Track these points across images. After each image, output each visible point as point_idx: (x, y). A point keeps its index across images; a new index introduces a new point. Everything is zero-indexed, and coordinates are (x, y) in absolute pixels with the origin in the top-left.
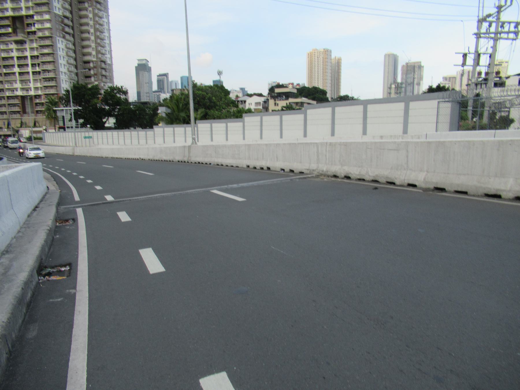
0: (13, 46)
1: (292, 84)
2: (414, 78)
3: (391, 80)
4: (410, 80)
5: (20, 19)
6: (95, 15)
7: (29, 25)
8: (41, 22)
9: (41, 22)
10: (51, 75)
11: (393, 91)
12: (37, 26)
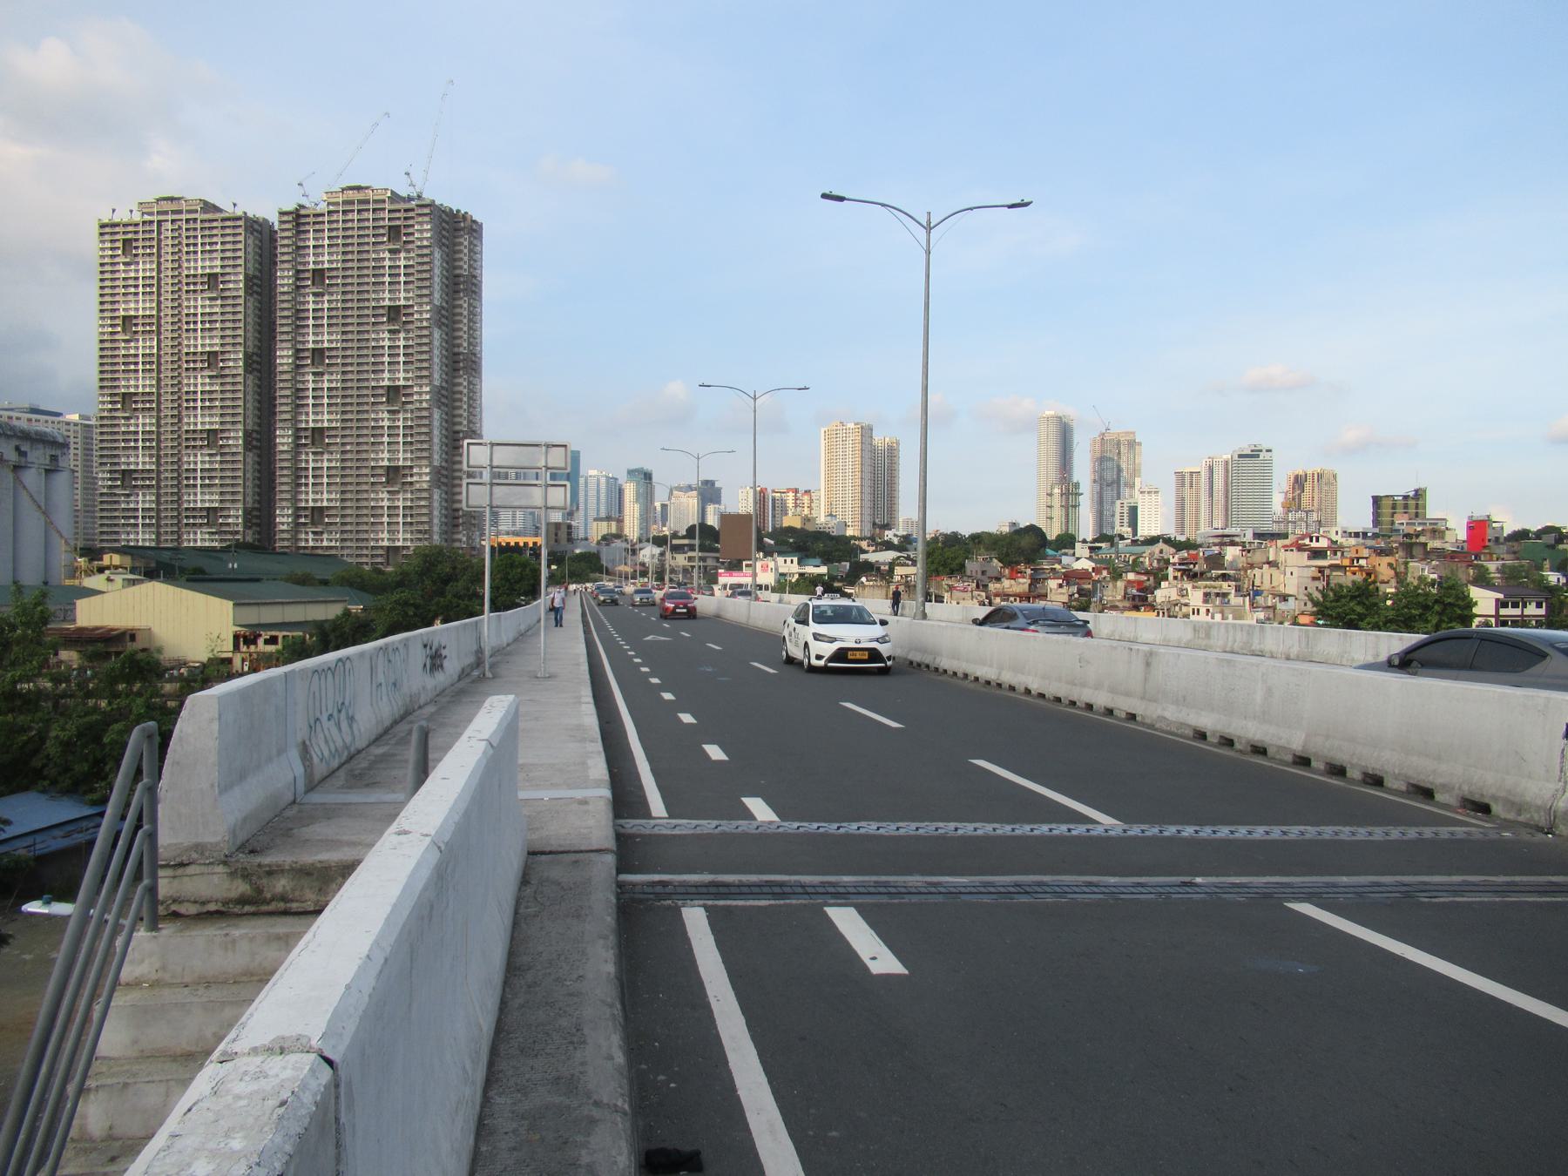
0: (385, 495)
1: (796, 491)
2: (1119, 470)
3: (1053, 474)
4: (1110, 476)
5: (397, 468)
7: (405, 476)
8: (420, 475)
9: (420, 475)
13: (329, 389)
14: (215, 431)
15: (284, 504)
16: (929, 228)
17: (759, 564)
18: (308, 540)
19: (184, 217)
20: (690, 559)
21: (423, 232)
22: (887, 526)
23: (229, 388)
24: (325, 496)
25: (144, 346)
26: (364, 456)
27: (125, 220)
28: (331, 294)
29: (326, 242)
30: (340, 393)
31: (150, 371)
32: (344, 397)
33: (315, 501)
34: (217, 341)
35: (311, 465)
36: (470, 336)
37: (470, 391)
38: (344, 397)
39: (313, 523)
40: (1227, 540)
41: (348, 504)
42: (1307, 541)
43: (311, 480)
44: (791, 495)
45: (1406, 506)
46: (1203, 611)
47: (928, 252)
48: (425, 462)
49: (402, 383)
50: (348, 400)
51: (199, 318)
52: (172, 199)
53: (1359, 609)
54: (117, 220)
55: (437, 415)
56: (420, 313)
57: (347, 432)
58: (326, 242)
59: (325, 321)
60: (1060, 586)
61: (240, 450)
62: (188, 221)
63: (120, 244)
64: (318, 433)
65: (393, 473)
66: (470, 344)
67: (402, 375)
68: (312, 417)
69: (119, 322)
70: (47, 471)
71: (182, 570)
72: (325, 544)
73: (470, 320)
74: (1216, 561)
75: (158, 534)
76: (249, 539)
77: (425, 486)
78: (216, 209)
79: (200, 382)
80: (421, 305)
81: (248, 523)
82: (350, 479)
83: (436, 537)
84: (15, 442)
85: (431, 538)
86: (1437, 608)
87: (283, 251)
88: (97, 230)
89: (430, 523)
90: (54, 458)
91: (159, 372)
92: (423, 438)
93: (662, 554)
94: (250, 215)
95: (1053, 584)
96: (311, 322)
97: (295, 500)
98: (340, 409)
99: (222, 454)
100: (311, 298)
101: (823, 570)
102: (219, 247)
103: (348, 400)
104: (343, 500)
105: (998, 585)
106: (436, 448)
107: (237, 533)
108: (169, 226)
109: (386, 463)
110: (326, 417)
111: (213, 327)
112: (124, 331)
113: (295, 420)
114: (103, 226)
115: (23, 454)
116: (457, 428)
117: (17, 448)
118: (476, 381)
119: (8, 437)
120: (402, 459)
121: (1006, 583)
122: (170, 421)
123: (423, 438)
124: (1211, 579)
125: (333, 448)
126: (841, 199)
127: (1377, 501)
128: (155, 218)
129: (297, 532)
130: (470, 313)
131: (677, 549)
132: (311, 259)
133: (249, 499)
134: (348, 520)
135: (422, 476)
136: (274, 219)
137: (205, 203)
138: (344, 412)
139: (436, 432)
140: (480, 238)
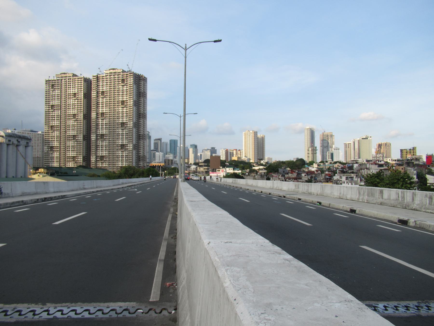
0: (120, 152)
1: (236, 150)
2: (328, 143)
3: (309, 145)
4: (325, 145)
5: (124, 145)
6: (143, 142)
9: (130, 146)
10: (131, 161)
11: (310, 152)
12: (128, 147)
13: (106, 123)
14: (75, 135)
15: (93, 155)
16: (186, 49)
17: (221, 170)
18: (100, 165)
19: (68, 78)
20: (204, 169)
21: (131, 80)
22: (262, 160)
23: (79, 124)
24: (104, 153)
25: (57, 113)
26: (115, 141)
27: (52, 79)
28: (106, 98)
29: (105, 84)
30: (108, 124)
31: (58, 119)
32: (109, 125)
33: (101, 154)
34: (76, 111)
35: (100, 144)
36: (144, 108)
37: (144, 123)
38: (109, 125)
39: (101, 160)
40: (355, 162)
41: (110, 155)
42: (378, 162)
43: (100, 148)
44: (235, 151)
45: (410, 152)
46: (346, 182)
47: (186, 57)
48: (131, 143)
49: (125, 121)
50: (110, 126)
51: (71, 105)
52: (65, 73)
53: (378, 180)
54: (50, 79)
55: (134, 130)
56: (130, 102)
57: (110, 135)
58: (105, 84)
59: (105, 105)
60: (305, 175)
61: (82, 140)
62: (69, 79)
63: (51, 86)
64: (102, 135)
65: (123, 146)
66: (144, 110)
67: (125, 119)
68: (101, 131)
69: (50, 106)
70: (26, 147)
71: (61, 173)
72: (104, 166)
73: (144, 104)
74: (351, 168)
75: (60, 164)
76: (84, 165)
77: (131, 149)
78: (76, 76)
79: (71, 122)
80: (130, 100)
81: (84, 160)
82: (111, 148)
83: (134, 164)
84: (17, 139)
85: (133, 164)
86: (401, 180)
87: (94, 86)
88: (45, 82)
89: (132, 159)
90: (27, 143)
91: (61, 120)
92: (131, 136)
93: (197, 168)
94: (85, 77)
95: (303, 175)
96: (101, 105)
97: (96, 154)
98: (108, 129)
99: (77, 142)
100: (101, 99)
101: (240, 171)
102: (77, 86)
103: (110, 126)
104: (109, 154)
105: (287, 175)
106: (134, 139)
107: (80, 163)
108: (64, 81)
109: (121, 143)
110: (105, 131)
111: (75, 107)
112: (52, 109)
113: (96, 132)
114: (46, 81)
115: (19, 142)
116: (140, 133)
117: (17, 140)
118: (145, 120)
119: (15, 137)
120: (125, 142)
121: (290, 175)
122: (63, 133)
123: (131, 136)
124: (349, 173)
125: (106, 139)
126: (155, 40)
127: (401, 151)
128: (60, 79)
129: (97, 163)
130: (144, 102)
131: (201, 166)
132: (101, 88)
133: (84, 154)
134: (110, 159)
135: (130, 147)
136: (91, 78)
137: (73, 74)
138: (109, 130)
139: (134, 135)
140: (146, 82)
